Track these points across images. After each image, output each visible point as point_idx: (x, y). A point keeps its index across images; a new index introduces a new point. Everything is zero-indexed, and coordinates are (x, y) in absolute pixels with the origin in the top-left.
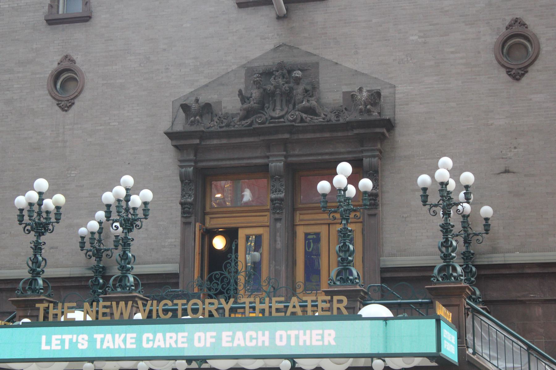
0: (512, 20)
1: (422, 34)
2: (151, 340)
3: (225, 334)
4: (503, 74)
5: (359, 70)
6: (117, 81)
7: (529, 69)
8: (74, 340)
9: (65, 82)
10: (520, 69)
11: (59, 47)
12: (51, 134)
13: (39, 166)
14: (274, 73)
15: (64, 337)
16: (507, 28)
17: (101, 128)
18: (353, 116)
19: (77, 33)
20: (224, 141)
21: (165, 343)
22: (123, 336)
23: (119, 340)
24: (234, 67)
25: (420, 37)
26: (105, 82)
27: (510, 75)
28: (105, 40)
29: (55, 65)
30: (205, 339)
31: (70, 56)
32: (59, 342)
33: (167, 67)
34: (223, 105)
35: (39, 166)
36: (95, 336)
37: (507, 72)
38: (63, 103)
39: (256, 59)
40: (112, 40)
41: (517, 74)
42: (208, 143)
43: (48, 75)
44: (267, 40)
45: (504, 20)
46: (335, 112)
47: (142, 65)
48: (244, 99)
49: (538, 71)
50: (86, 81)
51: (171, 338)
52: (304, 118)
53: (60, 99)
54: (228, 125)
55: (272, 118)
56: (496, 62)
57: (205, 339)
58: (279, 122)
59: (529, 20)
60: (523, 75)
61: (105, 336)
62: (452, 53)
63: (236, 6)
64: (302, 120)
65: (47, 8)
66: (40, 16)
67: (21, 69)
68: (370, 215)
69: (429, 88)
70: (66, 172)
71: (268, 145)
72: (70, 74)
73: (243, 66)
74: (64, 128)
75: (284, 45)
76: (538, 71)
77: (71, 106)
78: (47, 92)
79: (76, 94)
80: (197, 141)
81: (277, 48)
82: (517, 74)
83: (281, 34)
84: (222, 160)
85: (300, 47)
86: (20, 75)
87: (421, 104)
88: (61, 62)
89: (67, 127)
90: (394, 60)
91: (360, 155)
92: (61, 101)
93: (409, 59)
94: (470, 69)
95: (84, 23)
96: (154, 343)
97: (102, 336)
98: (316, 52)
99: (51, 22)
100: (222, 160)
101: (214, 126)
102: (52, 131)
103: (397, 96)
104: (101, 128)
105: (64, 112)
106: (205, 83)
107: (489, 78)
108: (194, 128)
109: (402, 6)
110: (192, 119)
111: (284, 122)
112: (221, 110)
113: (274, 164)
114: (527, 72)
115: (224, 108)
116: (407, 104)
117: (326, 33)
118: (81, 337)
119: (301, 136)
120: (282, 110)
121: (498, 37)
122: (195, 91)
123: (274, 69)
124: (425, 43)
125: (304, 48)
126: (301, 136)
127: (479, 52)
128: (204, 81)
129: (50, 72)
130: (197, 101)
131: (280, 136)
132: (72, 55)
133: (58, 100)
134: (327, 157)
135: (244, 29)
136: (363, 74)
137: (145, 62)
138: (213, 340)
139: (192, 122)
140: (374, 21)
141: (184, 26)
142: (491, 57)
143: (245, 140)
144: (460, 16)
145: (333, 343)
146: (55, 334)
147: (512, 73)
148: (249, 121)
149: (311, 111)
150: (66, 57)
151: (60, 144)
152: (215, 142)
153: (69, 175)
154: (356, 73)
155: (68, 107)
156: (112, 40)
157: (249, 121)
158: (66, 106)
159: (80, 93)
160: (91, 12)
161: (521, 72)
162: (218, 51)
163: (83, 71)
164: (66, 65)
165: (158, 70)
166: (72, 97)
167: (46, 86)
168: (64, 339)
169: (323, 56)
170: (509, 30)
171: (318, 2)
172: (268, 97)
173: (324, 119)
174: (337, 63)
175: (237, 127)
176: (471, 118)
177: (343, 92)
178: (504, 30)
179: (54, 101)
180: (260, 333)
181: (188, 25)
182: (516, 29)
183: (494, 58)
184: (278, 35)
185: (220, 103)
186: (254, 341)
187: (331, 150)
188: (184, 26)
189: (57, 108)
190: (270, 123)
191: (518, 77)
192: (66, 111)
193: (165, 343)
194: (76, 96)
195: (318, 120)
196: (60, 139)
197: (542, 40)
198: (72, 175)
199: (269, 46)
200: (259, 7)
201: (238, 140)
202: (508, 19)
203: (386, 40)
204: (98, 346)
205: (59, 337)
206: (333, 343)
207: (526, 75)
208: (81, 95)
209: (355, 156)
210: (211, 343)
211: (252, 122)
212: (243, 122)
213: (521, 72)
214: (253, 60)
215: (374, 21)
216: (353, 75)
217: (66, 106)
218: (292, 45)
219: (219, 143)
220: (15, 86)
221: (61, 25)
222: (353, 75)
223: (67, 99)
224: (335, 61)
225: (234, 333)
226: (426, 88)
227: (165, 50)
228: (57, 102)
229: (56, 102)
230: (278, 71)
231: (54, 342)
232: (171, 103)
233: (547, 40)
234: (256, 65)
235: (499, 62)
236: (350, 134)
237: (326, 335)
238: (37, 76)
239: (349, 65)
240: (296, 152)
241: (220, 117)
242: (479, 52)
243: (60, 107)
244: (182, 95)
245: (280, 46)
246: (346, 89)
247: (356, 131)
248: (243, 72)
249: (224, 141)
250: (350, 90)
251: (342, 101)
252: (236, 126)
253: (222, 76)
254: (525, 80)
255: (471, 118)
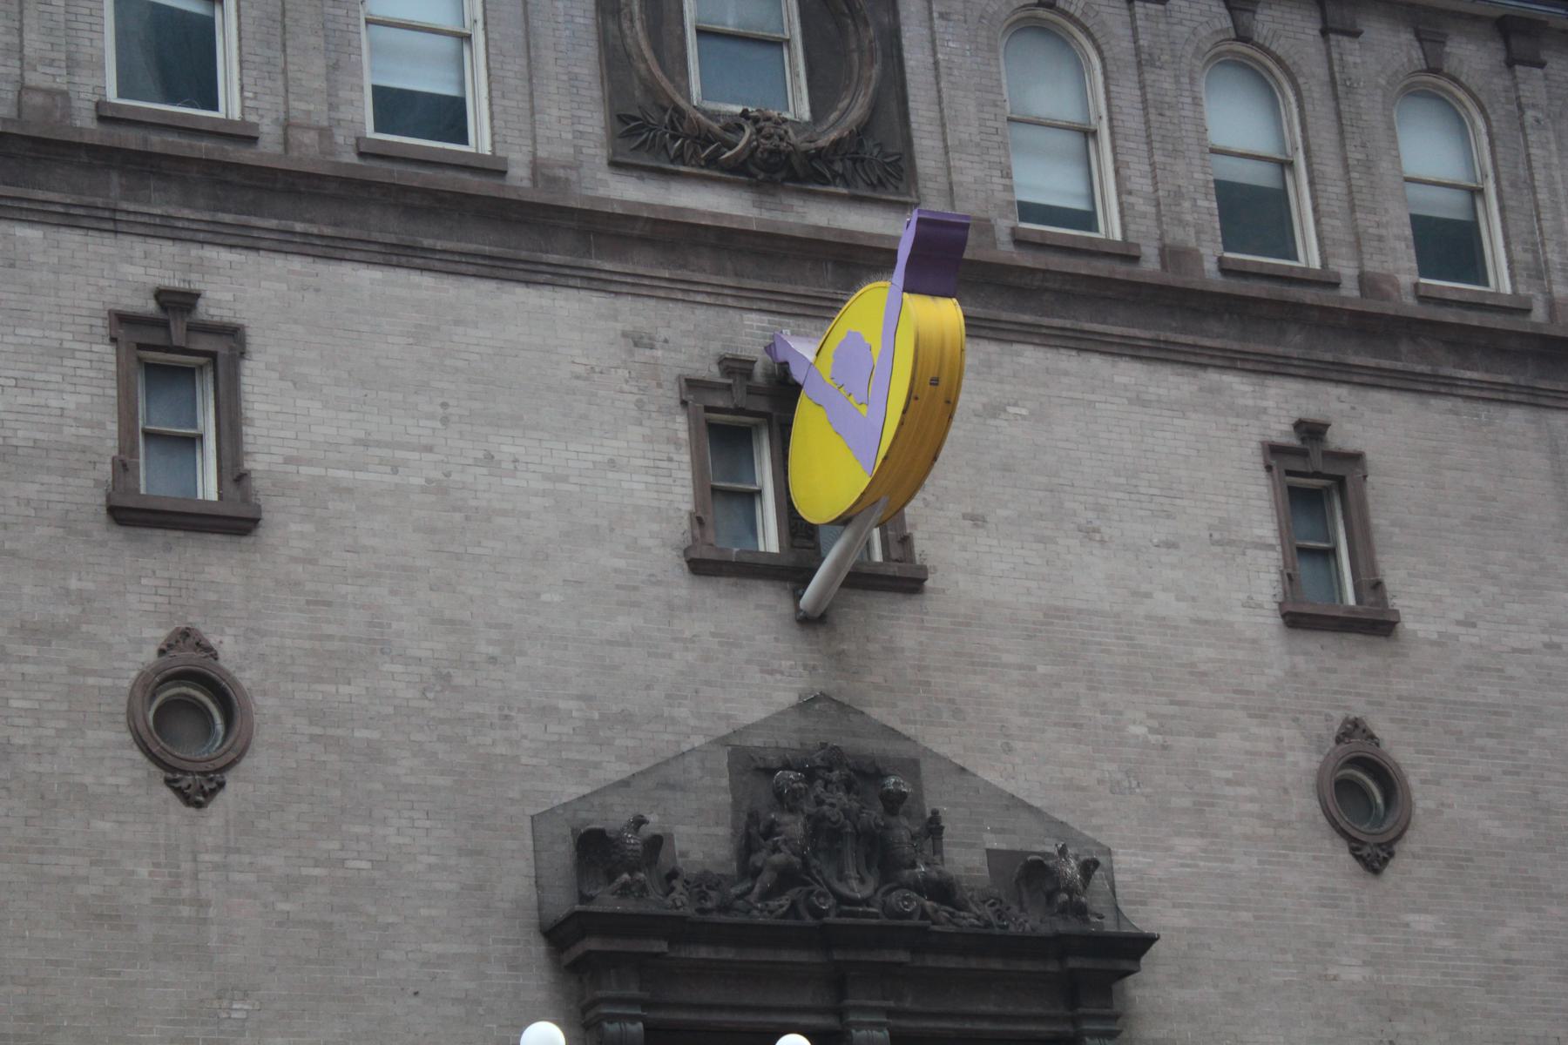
0: (1346, 721)
1: (1155, 723)
4: (1344, 856)
5: (1021, 795)
6: (357, 734)
7: (1396, 848)
9: (189, 715)
10: (1379, 845)
11: (159, 599)
12: (150, 874)
13: (118, 974)
14: (820, 772)
16: (1338, 740)
17: (317, 872)
18: (1031, 921)
19: (215, 566)
20: (728, 954)
24: (698, 741)
25: (1152, 730)
26: (318, 731)
27: (1358, 858)
28: (308, 603)
29: (149, 655)
31: (198, 633)
33: (506, 712)
34: (679, 845)
35: (118, 974)
37: (1353, 851)
38: (190, 778)
39: (754, 726)
40: (329, 604)
41: (1373, 858)
42: (683, 955)
43: (127, 684)
44: (778, 676)
45: (1328, 718)
46: (992, 905)
47: (431, 695)
48: (753, 836)
49: (1414, 856)
50: (257, 718)
52: (929, 910)
53: (177, 764)
54: (725, 908)
55: (841, 899)
56: (1322, 820)
58: (867, 915)
59: (1381, 726)
60: (1386, 860)
62: (1228, 782)
63: (686, 566)
64: (924, 915)
65: (106, 470)
66: (88, 490)
67: (31, 651)
69: (1188, 866)
70: (216, 1004)
71: (839, 982)
72: (184, 690)
73: (722, 741)
74: (195, 860)
75: (823, 697)
76: (1414, 856)
77: (213, 792)
78: (128, 737)
79: (232, 755)
80: (661, 946)
81: (806, 705)
82: (1373, 858)
83: (814, 668)
84: (710, 1007)
85: (867, 710)
86: (29, 669)
87: (1174, 906)
88: (169, 646)
89: (207, 857)
90: (1100, 782)
91: (1068, 1028)
92: (185, 772)
93: (1134, 784)
94: (1271, 831)
95: (235, 538)
98: (909, 730)
99: (129, 515)
100: (710, 1007)
101: (681, 902)
102: (156, 865)
103: (1118, 878)
104: (317, 872)
105: (191, 810)
106: (617, 778)
107: (1315, 858)
108: (629, 906)
109: (1100, 644)
110: (626, 876)
111: (876, 916)
112: (674, 860)
113: (864, 1032)
114: (1391, 854)
115: (683, 854)
116: (1144, 903)
117: (928, 683)
119: (931, 961)
120: (862, 881)
121: (1321, 758)
122: (594, 793)
123: (818, 762)
124: (1165, 747)
125: (877, 713)
126: (931, 961)
127: (1286, 791)
128: (615, 770)
129: (134, 674)
130: (640, 822)
131: (887, 956)
132: (203, 629)
133: (172, 769)
134: (986, 1026)
135: (713, 635)
136: (1030, 808)
137: (438, 688)
139: (625, 887)
140: (1041, 669)
141: (545, 597)
142: (1312, 806)
143: (786, 956)
144: (1235, 692)
147: (1366, 851)
148: (784, 902)
149: (943, 890)
150: (186, 633)
151: (186, 911)
152: (704, 953)
153: (224, 1015)
154: (1015, 804)
155: (205, 794)
156: (329, 604)
157: (784, 902)
158: (196, 788)
159: (241, 755)
160: (260, 512)
161: (1383, 854)
162: (648, 687)
163: (246, 684)
164: (186, 658)
165: (480, 716)
166: (219, 763)
167: (123, 718)
169: (930, 746)
170: (1343, 746)
171: (899, 596)
172: (824, 834)
173: (978, 918)
174: (963, 770)
175: (760, 919)
176: (1289, 957)
177: (988, 851)
178: (1332, 744)
179: (153, 768)
181: (557, 598)
182: (1357, 746)
183: (1319, 811)
184: (805, 667)
185: (671, 836)
187: (992, 1008)
188: (545, 597)
189: (167, 793)
190: (839, 916)
191: (1376, 865)
192: (199, 805)
194: (232, 763)
195: (968, 920)
196: (186, 892)
197: (1413, 781)
198: (235, 1015)
199: (786, 697)
200: (748, 582)
201: (766, 955)
202: (1339, 716)
203: (1075, 725)
207: (1391, 862)
208: (245, 763)
209: (1054, 1028)
211: (793, 905)
212: (773, 904)
213: (1383, 854)
214: (747, 727)
215: (1041, 669)
216: (1008, 808)
217: (196, 788)
218: (846, 700)
219: (713, 956)
220: (14, 703)
221: (159, 532)
222: (1008, 808)
223: (202, 767)
224: (958, 761)
226: (1182, 865)
227: (493, 660)
228: (170, 776)
229: (159, 774)
230: (830, 770)
232: (527, 824)
233: (1424, 782)
234: (757, 742)
235: (1334, 823)
236: (1052, 967)
238: (91, 681)
239: (992, 777)
240: (908, 1004)
241: (687, 882)
242: (1286, 791)
243: (179, 792)
244: (556, 802)
245: (814, 700)
246: (996, 843)
247: (1073, 963)
248: (722, 759)
249: (728, 954)
250: (1004, 847)
251: (986, 873)
252: (755, 912)
253: (667, 762)
254: (1391, 873)
255: (1289, 957)
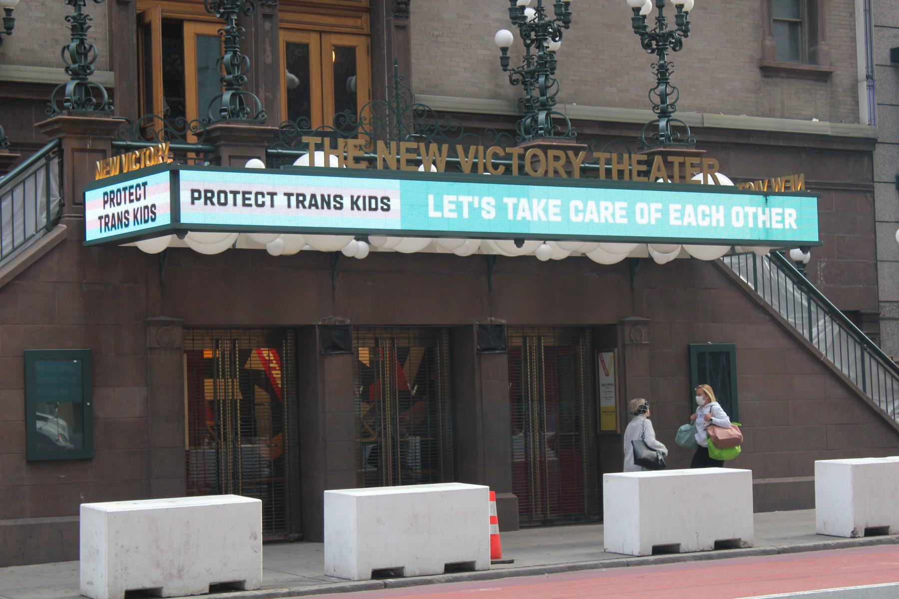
2: (580, 211)
3: (673, 207)
8: (476, 206)
15: (461, 198)
21: (599, 216)
22: (543, 202)
23: (538, 207)
30: (649, 214)
32: (453, 207)
36: (506, 200)
51: (606, 208)
57: (649, 214)
61: (519, 201)
68: (398, 27)
96: (584, 216)
97: (515, 200)
118: (486, 199)
138: (659, 215)
145: (795, 226)
146: (448, 194)
168: (462, 202)
180: (714, 208)
186: (707, 219)
193: (599, 216)
204: (510, 216)
205: (453, 198)
206: (795, 226)
210: (657, 219)
225: (684, 208)
231: (447, 206)
237: (786, 215)
